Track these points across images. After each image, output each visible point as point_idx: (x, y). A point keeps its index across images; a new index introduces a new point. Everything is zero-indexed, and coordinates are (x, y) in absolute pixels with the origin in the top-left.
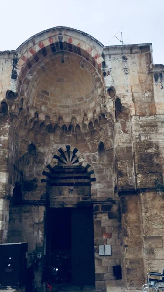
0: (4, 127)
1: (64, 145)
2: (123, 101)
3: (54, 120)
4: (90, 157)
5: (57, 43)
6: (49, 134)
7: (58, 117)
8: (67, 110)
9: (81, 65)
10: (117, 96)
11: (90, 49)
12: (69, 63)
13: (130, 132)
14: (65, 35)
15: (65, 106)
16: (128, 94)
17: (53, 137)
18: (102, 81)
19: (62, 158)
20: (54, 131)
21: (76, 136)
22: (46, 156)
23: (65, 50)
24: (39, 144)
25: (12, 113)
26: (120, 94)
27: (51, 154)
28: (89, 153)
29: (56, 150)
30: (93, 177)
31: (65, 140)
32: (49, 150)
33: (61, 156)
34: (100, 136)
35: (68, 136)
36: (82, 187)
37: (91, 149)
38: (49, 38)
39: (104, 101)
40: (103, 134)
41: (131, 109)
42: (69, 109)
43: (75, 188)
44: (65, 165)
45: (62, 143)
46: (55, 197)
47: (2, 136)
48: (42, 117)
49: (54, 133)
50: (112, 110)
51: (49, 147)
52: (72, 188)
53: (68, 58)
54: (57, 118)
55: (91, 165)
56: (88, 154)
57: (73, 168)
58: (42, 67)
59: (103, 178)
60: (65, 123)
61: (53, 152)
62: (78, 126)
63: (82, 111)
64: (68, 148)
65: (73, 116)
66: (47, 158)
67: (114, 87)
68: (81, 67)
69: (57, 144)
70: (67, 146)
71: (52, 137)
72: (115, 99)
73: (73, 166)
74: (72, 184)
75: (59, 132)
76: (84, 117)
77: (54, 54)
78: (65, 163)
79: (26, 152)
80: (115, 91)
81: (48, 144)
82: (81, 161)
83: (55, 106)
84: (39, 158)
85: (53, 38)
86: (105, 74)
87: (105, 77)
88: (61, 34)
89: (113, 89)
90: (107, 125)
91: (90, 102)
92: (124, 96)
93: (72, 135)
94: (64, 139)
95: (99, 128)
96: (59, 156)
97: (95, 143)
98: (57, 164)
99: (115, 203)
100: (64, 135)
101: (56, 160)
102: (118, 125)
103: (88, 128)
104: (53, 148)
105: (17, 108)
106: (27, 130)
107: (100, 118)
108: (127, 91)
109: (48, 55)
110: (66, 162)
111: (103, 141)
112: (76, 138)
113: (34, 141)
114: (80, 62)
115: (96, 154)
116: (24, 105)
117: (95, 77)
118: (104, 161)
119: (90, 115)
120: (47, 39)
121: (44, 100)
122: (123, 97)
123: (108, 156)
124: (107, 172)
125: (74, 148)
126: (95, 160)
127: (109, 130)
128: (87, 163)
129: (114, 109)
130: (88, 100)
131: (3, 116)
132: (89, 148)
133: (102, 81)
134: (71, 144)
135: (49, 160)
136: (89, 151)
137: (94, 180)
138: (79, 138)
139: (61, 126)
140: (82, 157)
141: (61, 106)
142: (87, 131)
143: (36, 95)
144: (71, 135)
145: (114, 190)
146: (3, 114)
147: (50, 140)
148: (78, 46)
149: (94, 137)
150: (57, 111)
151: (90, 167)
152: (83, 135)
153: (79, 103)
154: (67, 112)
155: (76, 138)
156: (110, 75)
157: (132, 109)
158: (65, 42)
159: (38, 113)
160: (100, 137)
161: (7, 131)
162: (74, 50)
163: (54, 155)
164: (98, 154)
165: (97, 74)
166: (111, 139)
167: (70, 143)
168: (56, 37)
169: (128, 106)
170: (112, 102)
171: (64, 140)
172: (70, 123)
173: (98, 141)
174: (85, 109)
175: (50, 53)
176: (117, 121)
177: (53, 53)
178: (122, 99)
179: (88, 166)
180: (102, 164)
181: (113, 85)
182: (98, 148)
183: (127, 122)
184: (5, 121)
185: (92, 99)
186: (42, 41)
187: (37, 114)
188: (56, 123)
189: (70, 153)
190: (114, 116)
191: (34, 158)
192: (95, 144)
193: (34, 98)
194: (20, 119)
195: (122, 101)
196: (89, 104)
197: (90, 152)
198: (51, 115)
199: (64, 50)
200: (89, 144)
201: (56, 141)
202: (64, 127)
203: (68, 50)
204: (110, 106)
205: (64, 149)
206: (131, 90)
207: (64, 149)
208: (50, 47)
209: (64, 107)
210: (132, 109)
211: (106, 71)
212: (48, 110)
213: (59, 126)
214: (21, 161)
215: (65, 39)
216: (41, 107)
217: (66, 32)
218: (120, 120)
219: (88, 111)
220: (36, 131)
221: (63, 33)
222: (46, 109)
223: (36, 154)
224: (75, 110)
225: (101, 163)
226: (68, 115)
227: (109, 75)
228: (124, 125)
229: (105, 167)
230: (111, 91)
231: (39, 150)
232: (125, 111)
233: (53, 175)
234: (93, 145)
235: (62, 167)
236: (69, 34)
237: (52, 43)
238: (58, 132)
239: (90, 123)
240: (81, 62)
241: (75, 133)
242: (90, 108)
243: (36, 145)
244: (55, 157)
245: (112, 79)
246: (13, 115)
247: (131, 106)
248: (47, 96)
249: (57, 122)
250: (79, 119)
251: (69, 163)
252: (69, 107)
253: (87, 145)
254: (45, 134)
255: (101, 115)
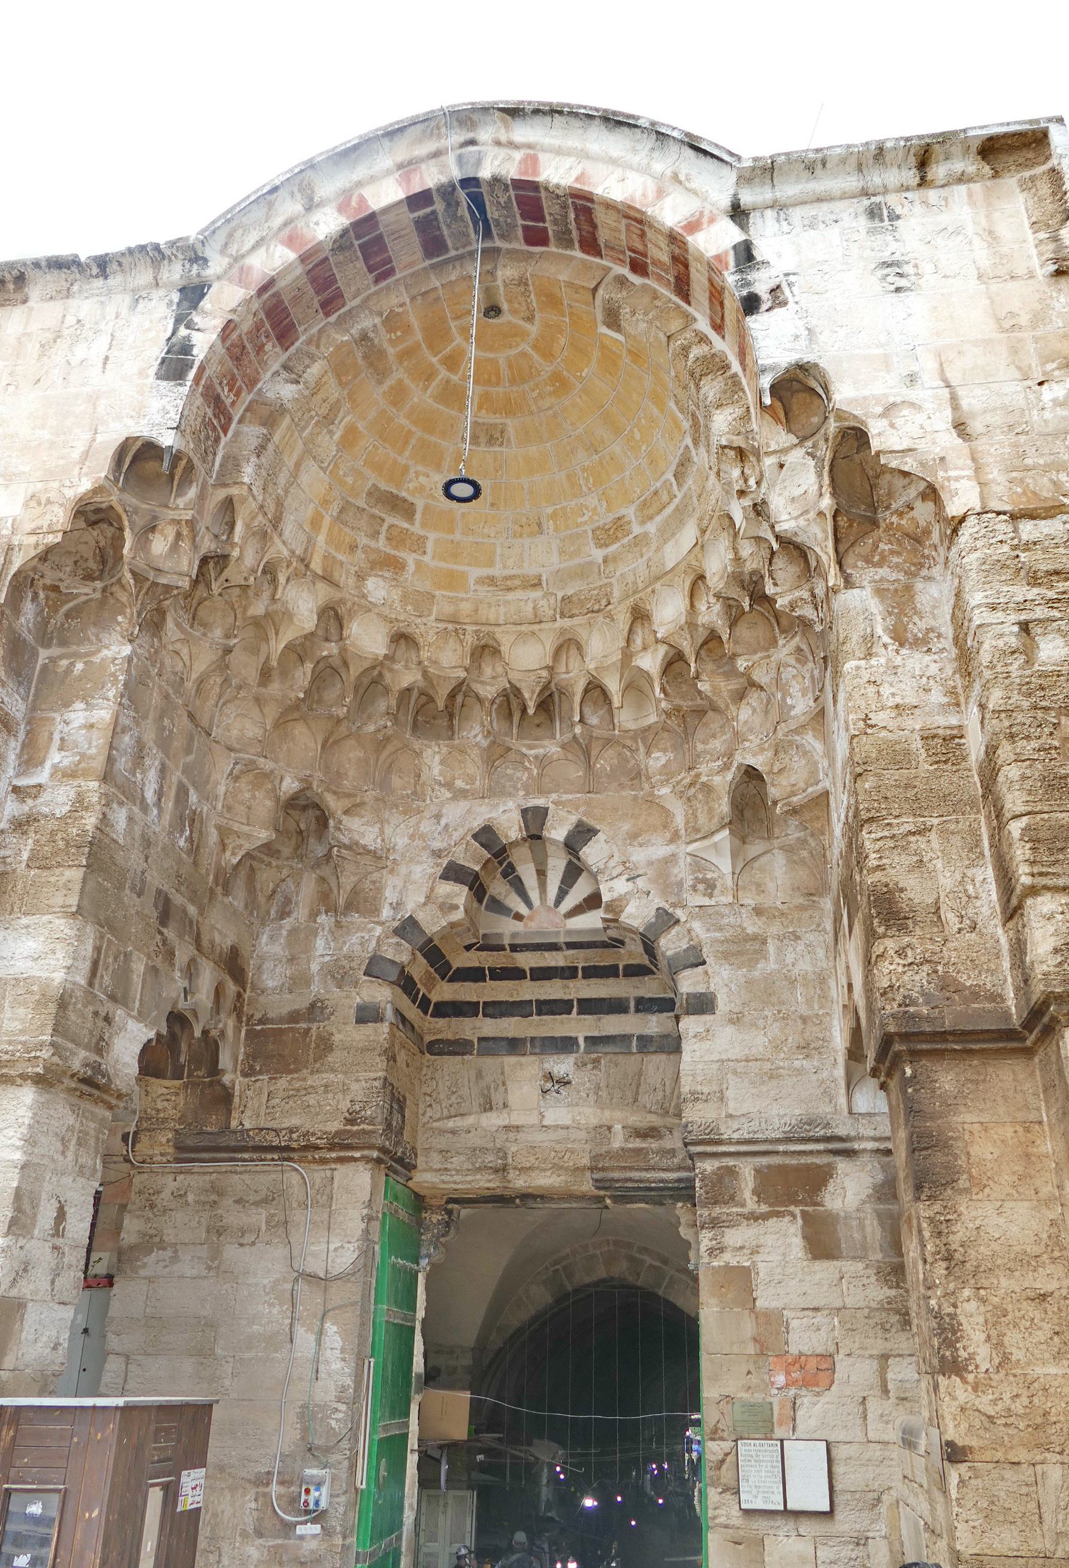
0: (96, 659)
1: (511, 804)
2: (884, 437)
3: (450, 660)
4: (675, 871)
5: (447, 191)
6: (417, 745)
7: (469, 639)
8: (525, 601)
9: (599, 316)
10: (840, 415)
11: (651, 195)
12: (530, 319)
13: (947, 643)
14: (498, 143)
15: (517, 582)
16: (913, 395)
17: (442, 762)
18: (736, 367)
19: (498, 888)
20: (451, 727)
21: (582, 751)
22: (392, 871)
23: (502, 237)
24: (349, 795)
25: (151, 575)
26: (865, 398)
27: (425, 856)
28: (672, 841)
29: (456, 836)
30: (701, 989)
31: (519, 774)
32: (412, 837)
33: (488, 869)
34: (736, 734)
35: (532, 752)
36: (631, 1063)
37: (679, 821)
38: (400, 166)
39: (752, 482)
40: (757, 720)
41: (949, 479)
42: (537, 594)
43: (580, 1065)
44: (519, 926)
45: (493, 792)
46: (450, 1124)
47: (79, 705)
48: (368, 638)
49: (451, 738)
50: (812, 515)
51: (413, 820)
52: (562, 1065)
53: (522, 282)
54: (468, 649)
55: (679, 913)
56: (659, 850)
57: (571, 945)
58: (364, 337)
59: (764, 993)
60: (514, 676)
61: (437, 845)
62: (596, 690)
63: (617, 594)
64: (535, 820)
65: (563, 631)
66: (400, 884)
67: (816, 365)
68: (604, 330)
69: (465, 797)
70: (524, 812)
71: (433, 758)
72: (827, 440)
73: (569, 932)
74: (566, 1045)
75: (477, 729)
76: (631, 631)
77: (433, 267)
78: (518, 917)
79: (264, 835)
80: (826, 389)
81: (411, 804)
82: (615, 895)
83: (453, 580)
84: (348, 881)
85: (423, 166)
86: (751, 304)
87: (748, 318)
88: (472, 142)
89: (813, 384)
90: (785, 649)
91: (668, 533)
92: (889, 410)
93: (563, 747)
94: (509, 771)
95: (728, 687)
96: (477, 868)
97: (704, 779)
98: (459, 915)
99: (850, 1154)
100: (509, 749)
101: (460, 894)
102: (860, 605)
103: (657, 690)
104: (443, 822)
105: (185, 545)
106: (272, 712)
107: (734, 616)
108: (912, 379)
109: (398, 275)
110: (523, 910)
111: (758, 762)
112: (589, 766)
113: (319, 775)
114: (595, 290)
115: (715, 845)
116: (236, 540)
117: (691, 356)
118: (771, 886)
119: (669, 611)
120: (388, 173)
121: (381, 543)
122: (884, 415)
123: (793, 863)
124: (790, 958)
125: (573, 819)
126: (710, 887)
127: (795, 688)
128: (658, 901)
129: (827, 502)
130: (651, 528)
131: (98, 595)
132: (667, 814)
133: (736, 367)
134: (554, 796)
135: (416, 890)
136: (668, 835)
137: (703, 1004)
138: (605, 762)
139: (488, 691)
140: (621, 868)
141: (491, 581)
142: (653, 719)
143: (335, 509)
144: (551, 748)
145: (840, 1072)
146: (99, 584)
147: (423, 778)
148: (578, 186)
149: (700, 747)
150: (466, 607)
151: (677, 928)
152: (629, 743)
153: (598, 554)
154: (528, 609)
155: (589, 766)
156: (791, 305)
157: (957, 479)
158: (496, 180)
159: (342, 610)
160: (738, 737)
161: (113, 675)
162: (555, 222)
163: (445, 862)
164: (727, 847)
165: (703, 339)
166: (811, 741)
167: (542, 791)
168: (443, 158)
169: (922, 464)
170: (812, 463)
171: (510, 778)
172: (545, 673)
173: (726, 767)
174: (635, 583)
175: (407, 254)
176: (849, 583)
177: (428, 262)
178: (875, 428)
179: (666, 920)
180: (758, 911)
181: (808, 357)
182: (724, 807)
183: (919, 585)
184: (103, 623)
185: (681, 515)
186: (359, 184)
187: (333, 617)
188: (463, 674)
189: (551, 849)
190: (824, 550)
191: (322, 880)
192: (707, 788)
193: (316, 523)
194: (218, 633)
195: (879, 434)
196: (658, 549)
197: (675, 837)
198: (426, 629)
199: (498, 243)
200: (665, 791)
201: (459, 783)
202: (509, 701)
203: (520, 232)
204: (798, 491)
205: (511, 829)
206: (942, 372)
207: (511, 829)
208: (409, 217)
209: (509, 583)
210: (957, 479)
211: (761, 289)
212: (405, 598)
213: (477, 697)
214: (227, 892)
215: (497, 163)
216: (361, 577)
217: (503, 130)
218: (866, 575)
219: (658, 586)
220: (331, 717)
221: (485, 134)
222: (396, 595)
223: (328, 856)
224: (574, 599)
225: (749, 900)
226: (536, 627)
227: (783, 304)
228: (900, 601)
229: (775, 929)
230: (798, 401)
231: (349, 830)
232: (901, 514)
233: (445, 992)
234: (697, 791)
235: (500, 936)
236: (524, 132)
237: (417, 189)
238: (474, 732)
239: (674, 662)
240: (601, 291)
241: (578, 730)
242: (670, 565)
243: (331, 802)
244: (453, 873)
245: (800, 324)
246: (155, 584)
247: (942, 459)
248: (406, 525)
249: (467, 670)
250: (601, 647)
251: (543, 912)
252: (537, 584)
253: (651, 801)
254: (387, 739)
255: (735, 592)
